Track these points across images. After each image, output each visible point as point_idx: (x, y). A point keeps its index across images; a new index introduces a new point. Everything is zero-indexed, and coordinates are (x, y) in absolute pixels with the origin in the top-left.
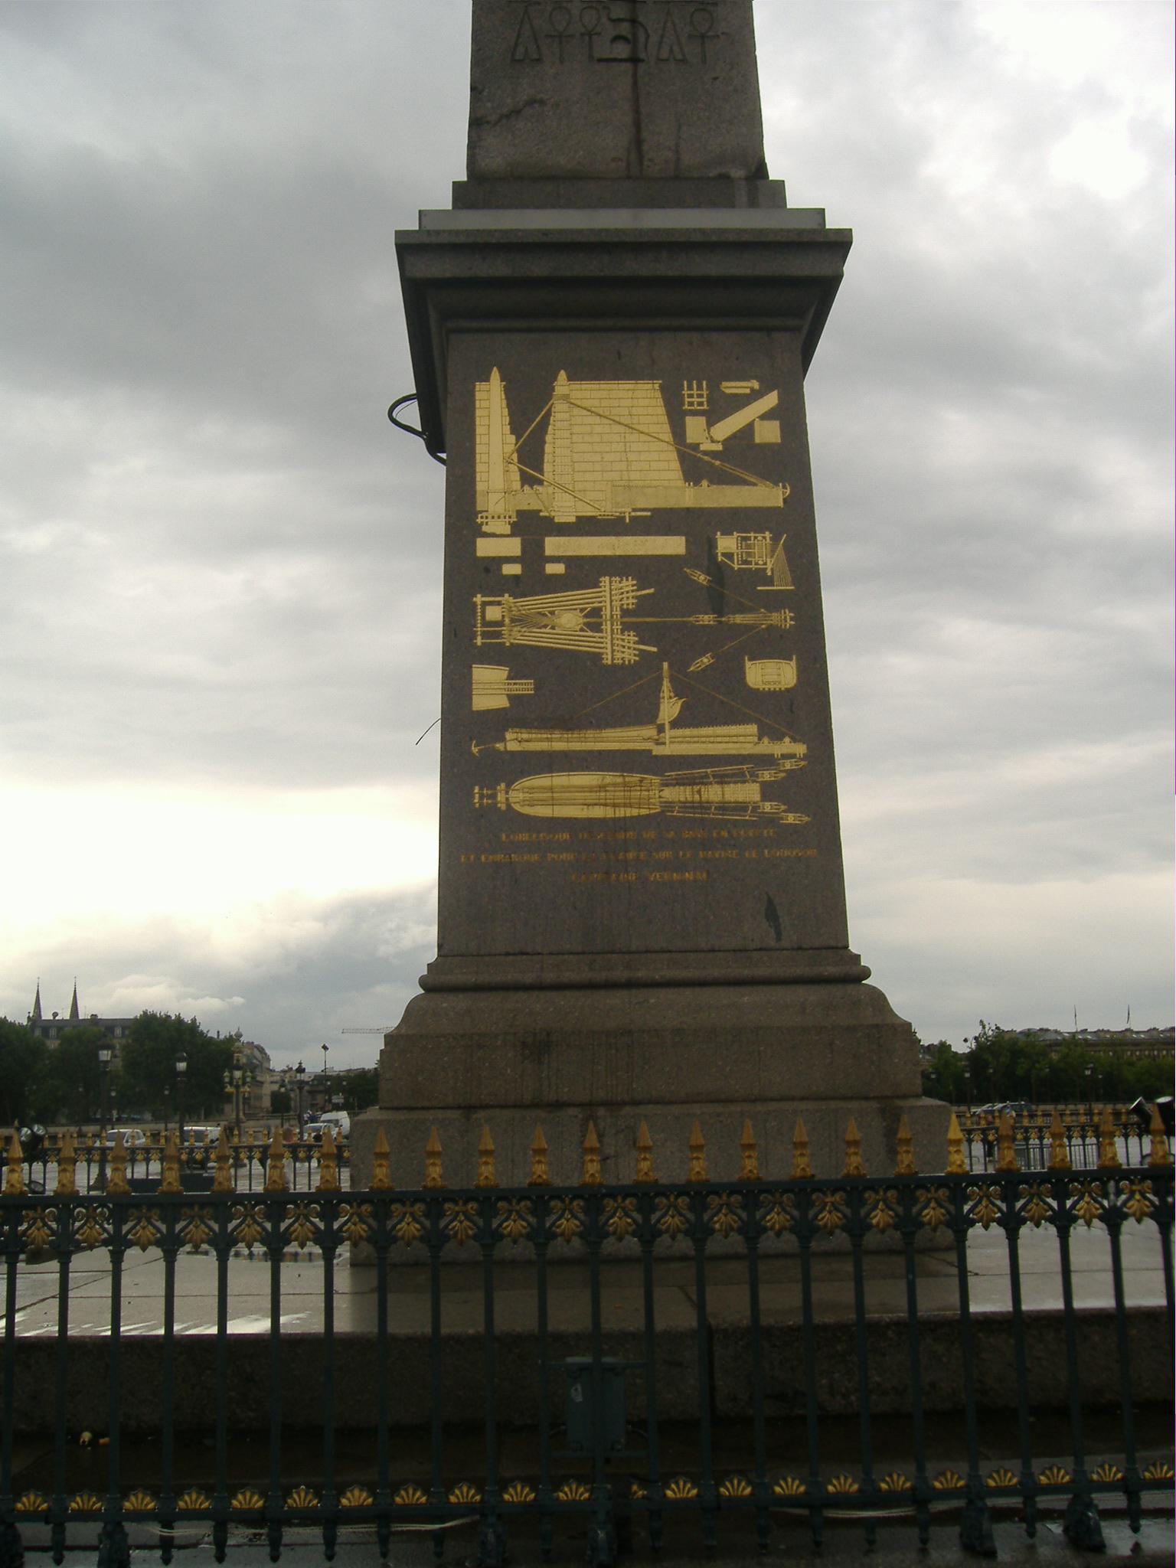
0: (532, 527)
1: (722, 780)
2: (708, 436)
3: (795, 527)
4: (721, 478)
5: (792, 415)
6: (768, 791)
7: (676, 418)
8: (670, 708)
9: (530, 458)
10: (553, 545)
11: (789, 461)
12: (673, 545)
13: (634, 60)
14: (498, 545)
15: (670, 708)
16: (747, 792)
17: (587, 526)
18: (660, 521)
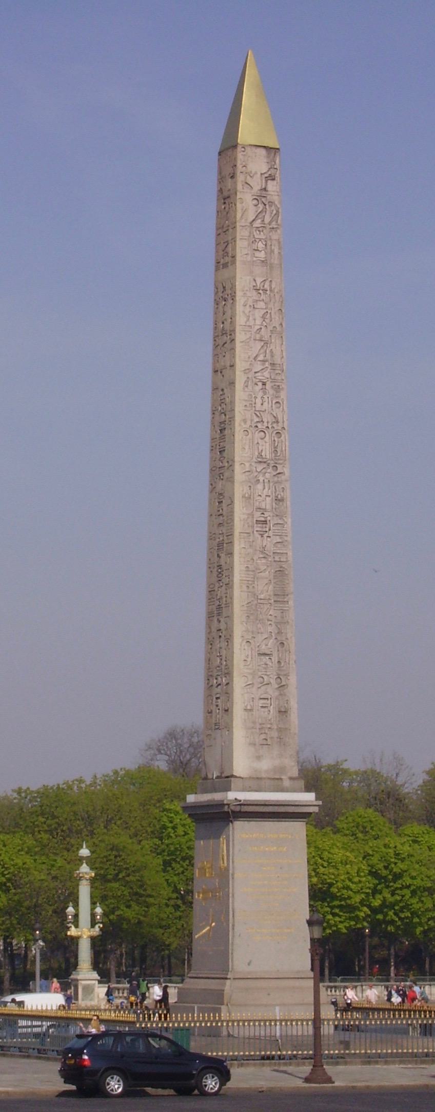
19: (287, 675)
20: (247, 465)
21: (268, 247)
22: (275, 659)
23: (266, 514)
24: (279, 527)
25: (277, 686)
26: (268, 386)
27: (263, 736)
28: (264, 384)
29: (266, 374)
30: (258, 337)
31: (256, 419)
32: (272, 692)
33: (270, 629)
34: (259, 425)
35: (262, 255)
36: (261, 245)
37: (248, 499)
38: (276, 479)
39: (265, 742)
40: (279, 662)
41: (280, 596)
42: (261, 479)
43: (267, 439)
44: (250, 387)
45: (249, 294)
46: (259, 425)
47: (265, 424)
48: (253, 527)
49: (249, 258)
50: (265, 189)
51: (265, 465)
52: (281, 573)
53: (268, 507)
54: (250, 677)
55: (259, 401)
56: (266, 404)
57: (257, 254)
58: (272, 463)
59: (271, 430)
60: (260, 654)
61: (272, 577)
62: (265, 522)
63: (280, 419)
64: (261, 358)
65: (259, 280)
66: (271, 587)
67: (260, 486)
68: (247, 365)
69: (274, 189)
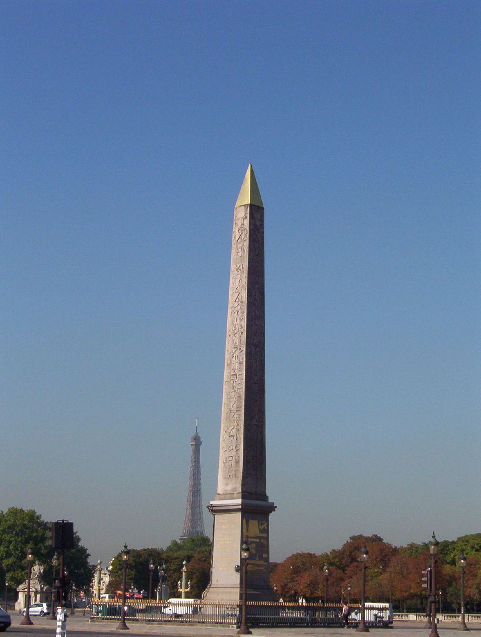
0: (247, 537)
1: (261, 567)
2: (262, 527)
3: (267, 538)
5: (268, 526)
6: (264, 568)
7: (259, 525)
8: (257, 559)
9: (247, 529)
11: (266, 531)
12: (258, 540)
13: (256, 478)
14: (244, 539)
15: (257, 559)
16: (263, 568)
17: (252, 537)
22: (235, 438)
27: (229, 474)
29: (239, 307)
32: (233, 453)
34: (235, 331)
35: (240, 254)
36: (240, 249)
37: (229, 365)
42: (234, 355)
50: (243, 224)
52: (240, 396)
53: (237, 368)
55: (235, 320)
56: (238, 320)
57: (239, 253)
66: (235, 405)
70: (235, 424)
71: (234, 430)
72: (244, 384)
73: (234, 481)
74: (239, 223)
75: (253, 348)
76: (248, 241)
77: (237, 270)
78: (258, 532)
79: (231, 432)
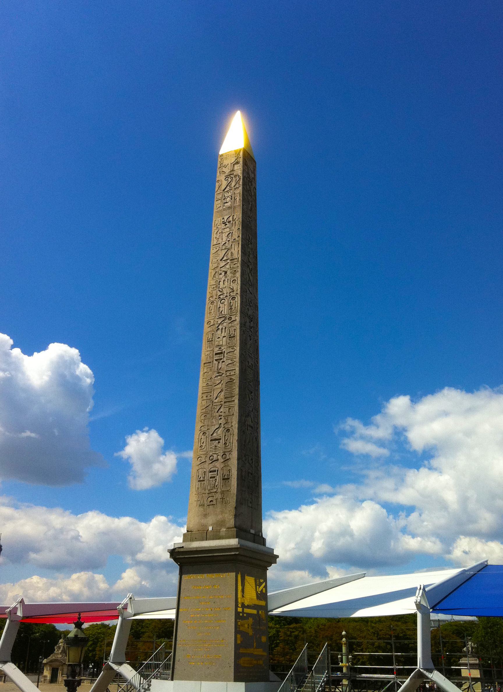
4: (261, 600)
5: (266, 587)
7: (256, 585)
10: (247, 610)
17: (248, 607)
18: (254, 607)
19: (230, 451)
20: (212, 321)
21: (233, 198)
22: (222, 441)
23: (223, 348)
24: (231, 354)
25: (223, 461)
26: (228, 273)
27: (210, 499)
28: (226, 273)
30: (224, 247)
31: (219, 293)
32: (219, 465)
33: (220, 422)
35: (229, 204)
36: (229, 199)
37: (210, 341)
38: (230, 325)
39: (211, 503)
40: (225, 443)
41: (228, 399)
42: (220, 327)
43: (226, 303)
44: (217, 277)
45: (219, 227)
46: (221, 297)
47: (225, 295)
48: (213, 358)
49: (221, 208)
50: (233, 170)
51: (223, 319)
53: (224, 343)
54: (204, 457)
56: (226, 283)
57: (226, 204)
58: (228, 316)
59: (228, 298)
60: (211, 440)
61: (224, 386)
62: (221, 353)
63: (235, 289)
64: (225, 259)
65: (226, 218)
67: (219, 332)
68: (216, 265)
69: (239, 168)
70: (222, 421)
71: (220, 431)
72: (238, 365)
73: (218, 510)
74: (227, 171)
75: (248, 320)
76: (241, 188)
77: (224, 223)
78: (254, 596)
79: (215, 434)
